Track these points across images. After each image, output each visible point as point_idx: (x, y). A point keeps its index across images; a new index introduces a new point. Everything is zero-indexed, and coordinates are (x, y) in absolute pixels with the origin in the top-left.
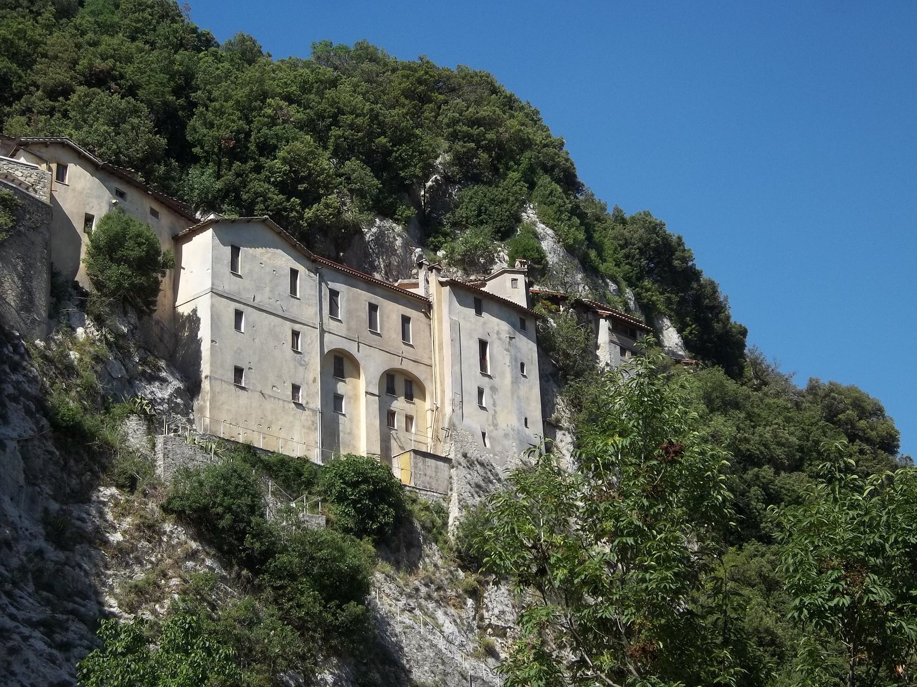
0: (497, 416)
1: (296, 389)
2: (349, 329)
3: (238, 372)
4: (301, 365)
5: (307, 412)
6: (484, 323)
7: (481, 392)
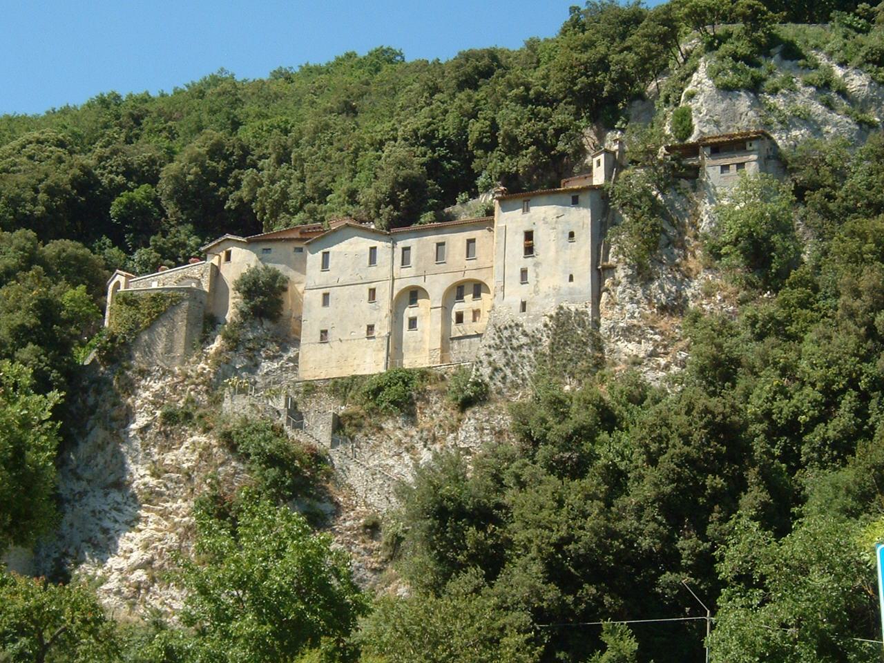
0: (539, 284)
1: (371, 328)
2: (417, 270)
3: (324, 333)
4: (376, 310)
5: (377, 340)
6: (531, 216)
7: (524, 273)
